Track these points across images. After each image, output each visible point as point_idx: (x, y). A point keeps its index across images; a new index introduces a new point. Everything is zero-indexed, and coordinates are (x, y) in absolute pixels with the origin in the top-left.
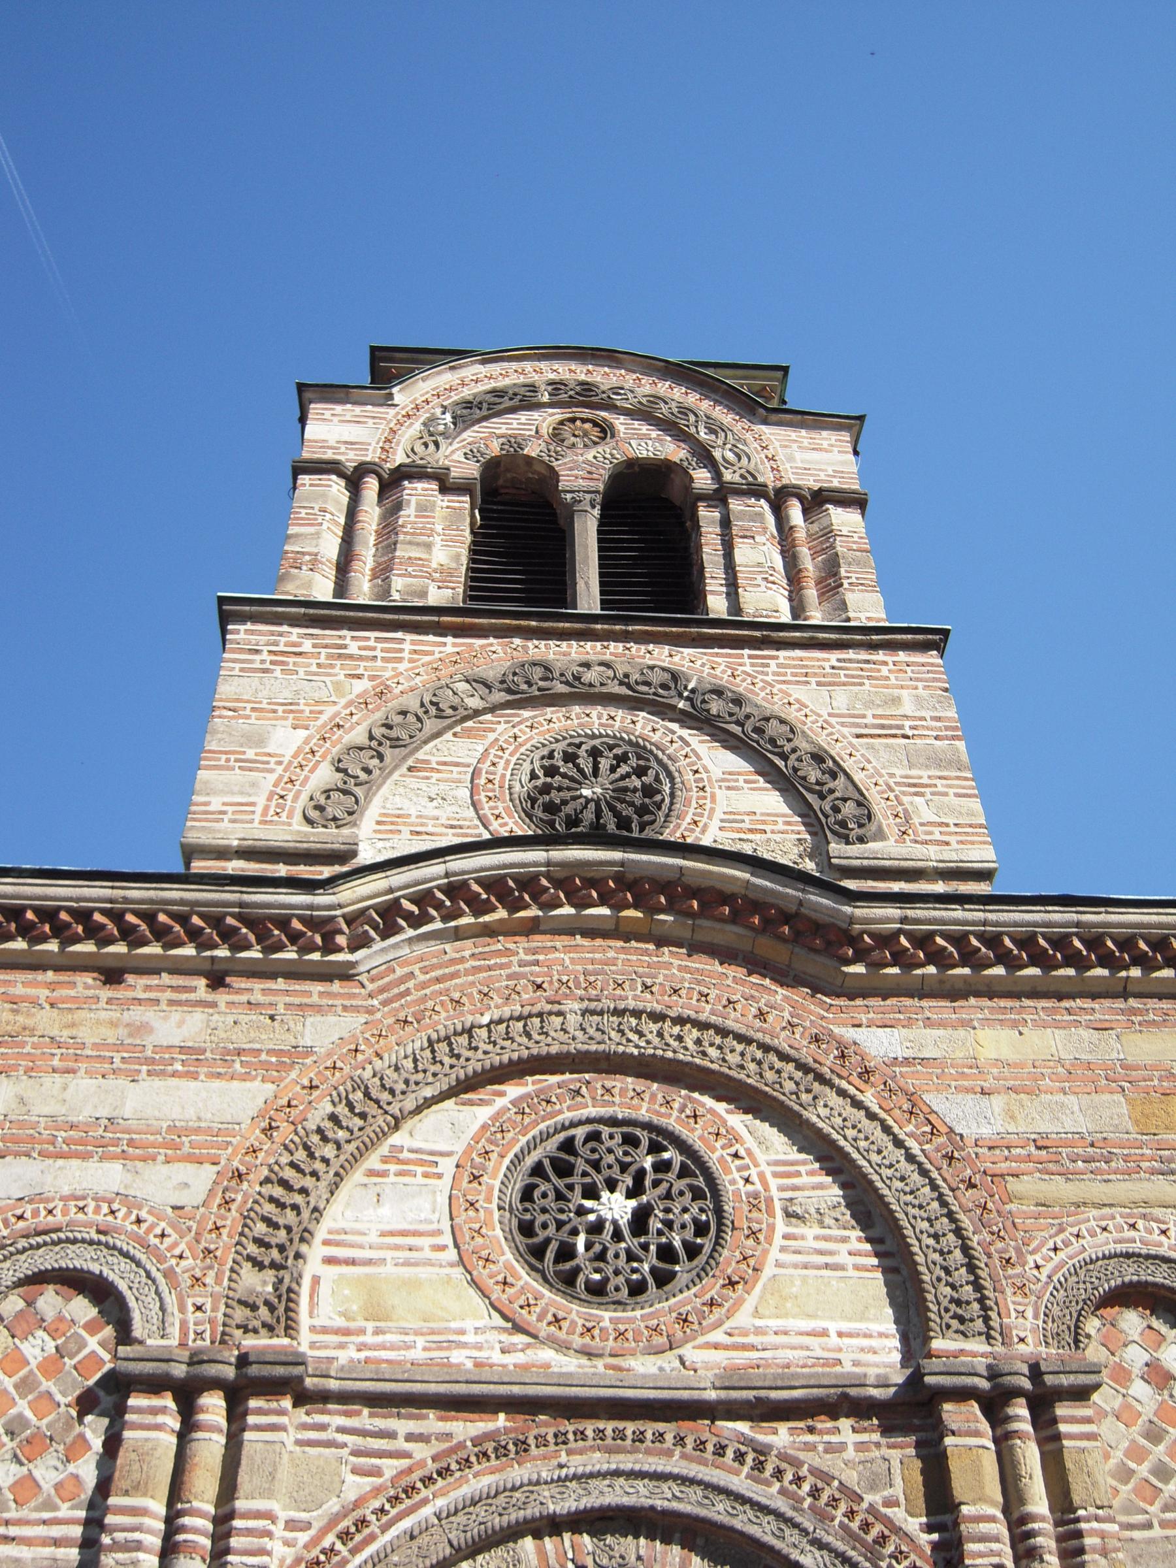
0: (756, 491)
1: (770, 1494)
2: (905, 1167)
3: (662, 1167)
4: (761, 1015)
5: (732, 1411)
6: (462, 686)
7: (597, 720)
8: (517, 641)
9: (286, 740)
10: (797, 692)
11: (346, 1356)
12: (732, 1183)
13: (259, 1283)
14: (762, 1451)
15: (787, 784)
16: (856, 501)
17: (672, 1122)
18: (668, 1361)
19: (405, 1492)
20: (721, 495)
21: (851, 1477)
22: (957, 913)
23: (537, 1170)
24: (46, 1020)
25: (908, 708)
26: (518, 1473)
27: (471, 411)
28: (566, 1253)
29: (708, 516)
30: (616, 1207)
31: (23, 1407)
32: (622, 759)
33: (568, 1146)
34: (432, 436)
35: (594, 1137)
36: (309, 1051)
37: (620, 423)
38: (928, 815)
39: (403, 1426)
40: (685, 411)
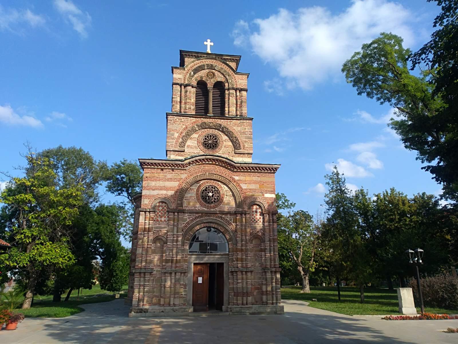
0: (233, 89)
1: (222, 221)
2: (237, 191)
3: (215, 190)
4: (226, 174)
5: (219, 214)
6: (196, 126)
7: (211, 131)
8: (202, 119)
9: (176, 135)
10: (234, 128)
11: (187, 209)
12: (221, 193)
13: (179, 202)
14: (222, 217)
15: (232, 141)
16: (246, 90)
17: (216, 186)
18: (215, 209)
19: (192, 220)
20: (229, 89)
21: (229, 220)
22: (245, 165)
23: (204, 190)
24: (156, 175)
25: (247, 130)
26: (201, 219)
27: (196, 71)
28: (206, 199)
29: (227, 92)
30: (211, 194)
31: (160, 214)
32: (214, 137)
33: (206, 188)
34: (191, 77)
35: (209, 187)
36: (182, 179)
37: (216, 73)
38: (246, 146)
39: (192, 215)
40: (225, 71)
